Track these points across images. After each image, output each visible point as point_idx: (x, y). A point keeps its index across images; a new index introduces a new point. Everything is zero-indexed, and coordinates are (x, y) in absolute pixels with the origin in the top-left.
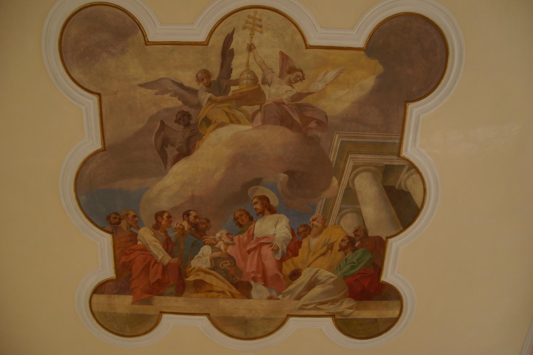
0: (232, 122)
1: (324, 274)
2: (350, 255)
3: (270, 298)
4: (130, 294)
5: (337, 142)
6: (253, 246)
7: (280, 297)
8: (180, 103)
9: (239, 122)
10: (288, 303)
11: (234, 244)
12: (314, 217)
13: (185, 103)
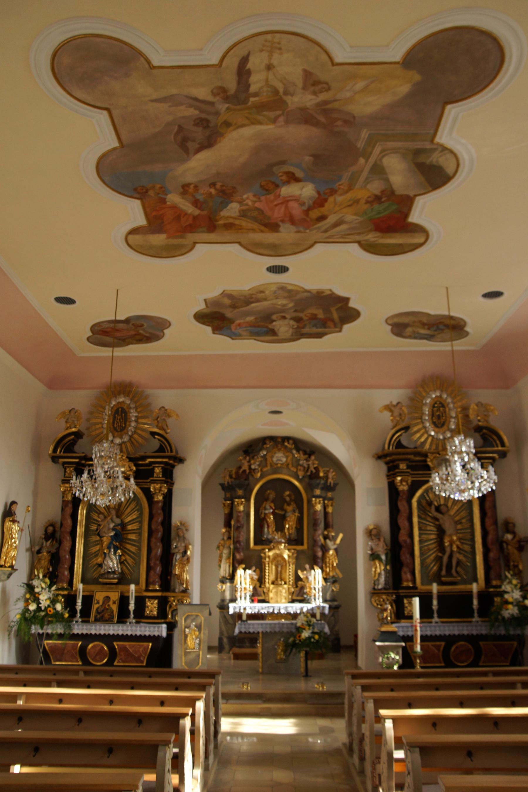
0: (253, 123)
1: (349, 217)
2: (376, 206)
3: (298, 232)
4: (164, 233)
5: (365, 134)
6: (280, 202)
7: (308, 231)
8: (197, 112)
9: (260, 123)
10: (314, 235)
11: (261, 201)
12: (340, 183)
13: (202, 111)
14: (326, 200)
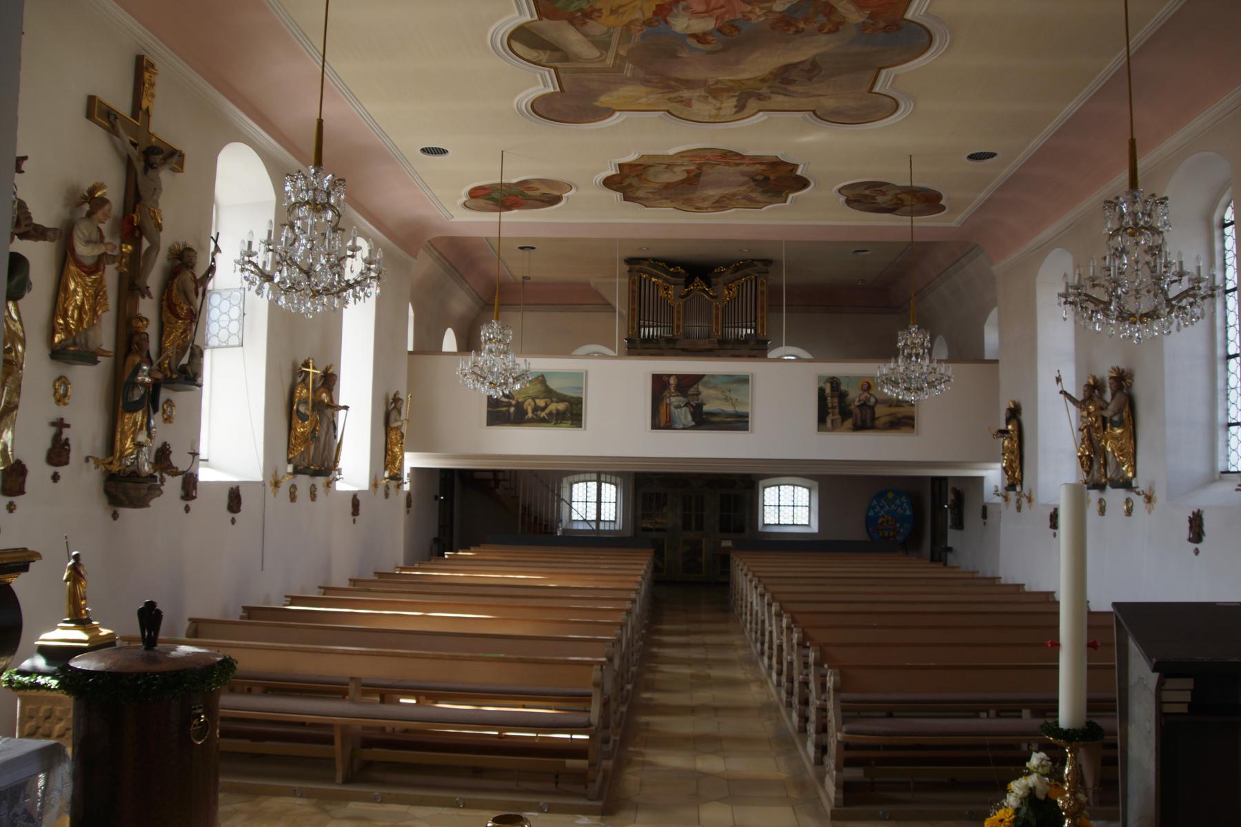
2: (585, 6)
14: (655, 13)
